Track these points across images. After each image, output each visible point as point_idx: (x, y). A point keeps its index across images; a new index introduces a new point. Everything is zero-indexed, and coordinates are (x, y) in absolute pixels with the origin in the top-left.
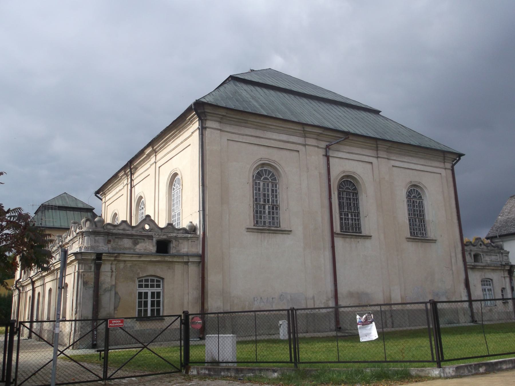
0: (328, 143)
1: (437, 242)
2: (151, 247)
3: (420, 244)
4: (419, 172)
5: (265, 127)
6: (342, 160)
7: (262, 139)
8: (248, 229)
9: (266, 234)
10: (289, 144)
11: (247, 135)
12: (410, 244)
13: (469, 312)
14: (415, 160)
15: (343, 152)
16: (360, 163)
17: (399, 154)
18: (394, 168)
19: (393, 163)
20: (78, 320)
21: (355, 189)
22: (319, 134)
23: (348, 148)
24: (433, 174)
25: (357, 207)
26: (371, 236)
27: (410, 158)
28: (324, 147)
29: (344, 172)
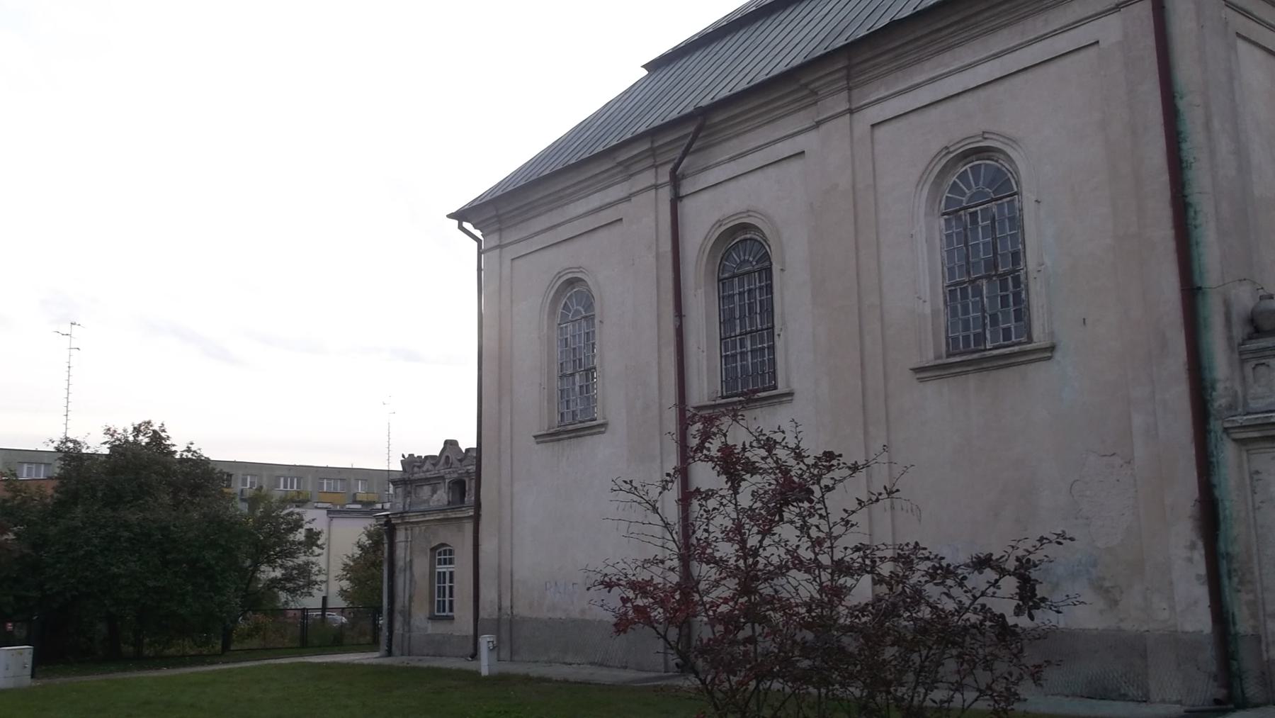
0: (670, 166)
1: (1058, 355)
2: (442, 496)
3: (972, 380)
4: (982, 93)
5: (561, 198)
6: (720, 189)
7: (560, 229)
8: (535, 437)
9: (566, 442)
10: (603, 214)
11: (537, 234)
12: (931, 388)
13: (1208, 656)
14: (964, 55)
15: (718, 164)
16: (770, 170)
17: (899, 68)
18: (881, 132)
19: (874, 114)
20: (323, 615)
21: (766, 257)
22: (653, 152)
23: (733, 147)
24: (1052, 67)
25: (768, 310)
26: (790, 394)
27: (947, 56)
28: (667, 179)
29: (719, 223)
